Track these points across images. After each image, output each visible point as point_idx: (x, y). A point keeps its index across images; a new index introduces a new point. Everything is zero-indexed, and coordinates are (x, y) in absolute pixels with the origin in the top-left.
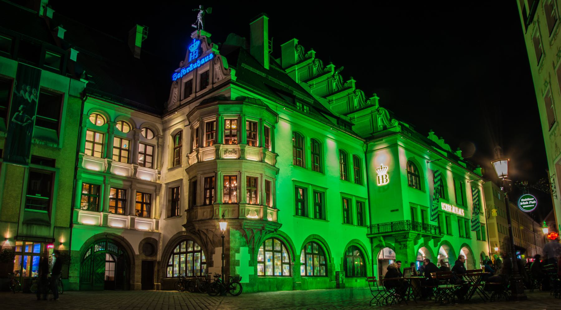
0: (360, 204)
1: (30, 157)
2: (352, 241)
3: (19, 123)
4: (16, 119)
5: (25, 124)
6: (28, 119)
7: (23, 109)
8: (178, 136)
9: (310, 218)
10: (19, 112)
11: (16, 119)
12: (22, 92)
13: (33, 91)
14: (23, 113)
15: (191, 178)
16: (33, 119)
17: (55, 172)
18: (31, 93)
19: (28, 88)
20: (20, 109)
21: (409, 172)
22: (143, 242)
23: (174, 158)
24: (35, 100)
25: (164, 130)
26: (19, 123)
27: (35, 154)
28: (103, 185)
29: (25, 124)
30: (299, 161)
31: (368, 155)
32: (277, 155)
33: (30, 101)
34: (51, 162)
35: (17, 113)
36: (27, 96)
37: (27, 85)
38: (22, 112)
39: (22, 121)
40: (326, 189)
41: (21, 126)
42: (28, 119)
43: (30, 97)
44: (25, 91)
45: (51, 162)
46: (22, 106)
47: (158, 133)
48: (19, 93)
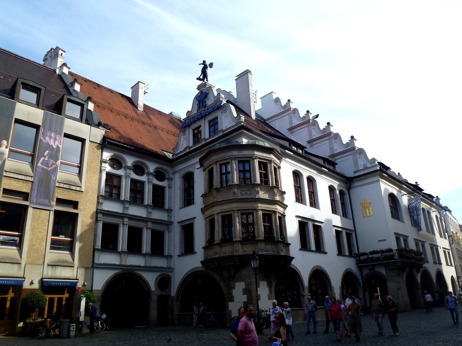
1: (55, 200)
2: (347, 269)
3: (45, 167)
4: (42, 163)
5: (51, 168)
6: (53, 164)
7: (48, 155)
8: (189, 179)
9: (312, 251)
10: (45, 157)
11: (42, 163)
12: (47, 138)
13: (57, 138)
14: (48, 158)
16: (57, 163)
17: (78, 214)
18: (55, 139)
19: (53, 135)
20: (46, 154)
21: (390, 206)
22: (159, 279)
23: (185, 198)
24: (59, 146)
25: (174, 173)
26: (45, 167)
27: (60, 197)
28: (122, 224)
29: (51, 168)
30: (299, 199)
31: (351, 191)
32: (284, 193)
33: (55, 147)
34: (75, 204)
35: (43, 158)
36: (52, 142)
37: (52, 132)
38: (47, 157)
39: (47, 166)
41: (47, 170)
42: (53, 164)
43: (54, 143)
44: (51, 137)
45: (75, 204)
46: (47, 152)
47: (168, 175)
48: (45, 139)
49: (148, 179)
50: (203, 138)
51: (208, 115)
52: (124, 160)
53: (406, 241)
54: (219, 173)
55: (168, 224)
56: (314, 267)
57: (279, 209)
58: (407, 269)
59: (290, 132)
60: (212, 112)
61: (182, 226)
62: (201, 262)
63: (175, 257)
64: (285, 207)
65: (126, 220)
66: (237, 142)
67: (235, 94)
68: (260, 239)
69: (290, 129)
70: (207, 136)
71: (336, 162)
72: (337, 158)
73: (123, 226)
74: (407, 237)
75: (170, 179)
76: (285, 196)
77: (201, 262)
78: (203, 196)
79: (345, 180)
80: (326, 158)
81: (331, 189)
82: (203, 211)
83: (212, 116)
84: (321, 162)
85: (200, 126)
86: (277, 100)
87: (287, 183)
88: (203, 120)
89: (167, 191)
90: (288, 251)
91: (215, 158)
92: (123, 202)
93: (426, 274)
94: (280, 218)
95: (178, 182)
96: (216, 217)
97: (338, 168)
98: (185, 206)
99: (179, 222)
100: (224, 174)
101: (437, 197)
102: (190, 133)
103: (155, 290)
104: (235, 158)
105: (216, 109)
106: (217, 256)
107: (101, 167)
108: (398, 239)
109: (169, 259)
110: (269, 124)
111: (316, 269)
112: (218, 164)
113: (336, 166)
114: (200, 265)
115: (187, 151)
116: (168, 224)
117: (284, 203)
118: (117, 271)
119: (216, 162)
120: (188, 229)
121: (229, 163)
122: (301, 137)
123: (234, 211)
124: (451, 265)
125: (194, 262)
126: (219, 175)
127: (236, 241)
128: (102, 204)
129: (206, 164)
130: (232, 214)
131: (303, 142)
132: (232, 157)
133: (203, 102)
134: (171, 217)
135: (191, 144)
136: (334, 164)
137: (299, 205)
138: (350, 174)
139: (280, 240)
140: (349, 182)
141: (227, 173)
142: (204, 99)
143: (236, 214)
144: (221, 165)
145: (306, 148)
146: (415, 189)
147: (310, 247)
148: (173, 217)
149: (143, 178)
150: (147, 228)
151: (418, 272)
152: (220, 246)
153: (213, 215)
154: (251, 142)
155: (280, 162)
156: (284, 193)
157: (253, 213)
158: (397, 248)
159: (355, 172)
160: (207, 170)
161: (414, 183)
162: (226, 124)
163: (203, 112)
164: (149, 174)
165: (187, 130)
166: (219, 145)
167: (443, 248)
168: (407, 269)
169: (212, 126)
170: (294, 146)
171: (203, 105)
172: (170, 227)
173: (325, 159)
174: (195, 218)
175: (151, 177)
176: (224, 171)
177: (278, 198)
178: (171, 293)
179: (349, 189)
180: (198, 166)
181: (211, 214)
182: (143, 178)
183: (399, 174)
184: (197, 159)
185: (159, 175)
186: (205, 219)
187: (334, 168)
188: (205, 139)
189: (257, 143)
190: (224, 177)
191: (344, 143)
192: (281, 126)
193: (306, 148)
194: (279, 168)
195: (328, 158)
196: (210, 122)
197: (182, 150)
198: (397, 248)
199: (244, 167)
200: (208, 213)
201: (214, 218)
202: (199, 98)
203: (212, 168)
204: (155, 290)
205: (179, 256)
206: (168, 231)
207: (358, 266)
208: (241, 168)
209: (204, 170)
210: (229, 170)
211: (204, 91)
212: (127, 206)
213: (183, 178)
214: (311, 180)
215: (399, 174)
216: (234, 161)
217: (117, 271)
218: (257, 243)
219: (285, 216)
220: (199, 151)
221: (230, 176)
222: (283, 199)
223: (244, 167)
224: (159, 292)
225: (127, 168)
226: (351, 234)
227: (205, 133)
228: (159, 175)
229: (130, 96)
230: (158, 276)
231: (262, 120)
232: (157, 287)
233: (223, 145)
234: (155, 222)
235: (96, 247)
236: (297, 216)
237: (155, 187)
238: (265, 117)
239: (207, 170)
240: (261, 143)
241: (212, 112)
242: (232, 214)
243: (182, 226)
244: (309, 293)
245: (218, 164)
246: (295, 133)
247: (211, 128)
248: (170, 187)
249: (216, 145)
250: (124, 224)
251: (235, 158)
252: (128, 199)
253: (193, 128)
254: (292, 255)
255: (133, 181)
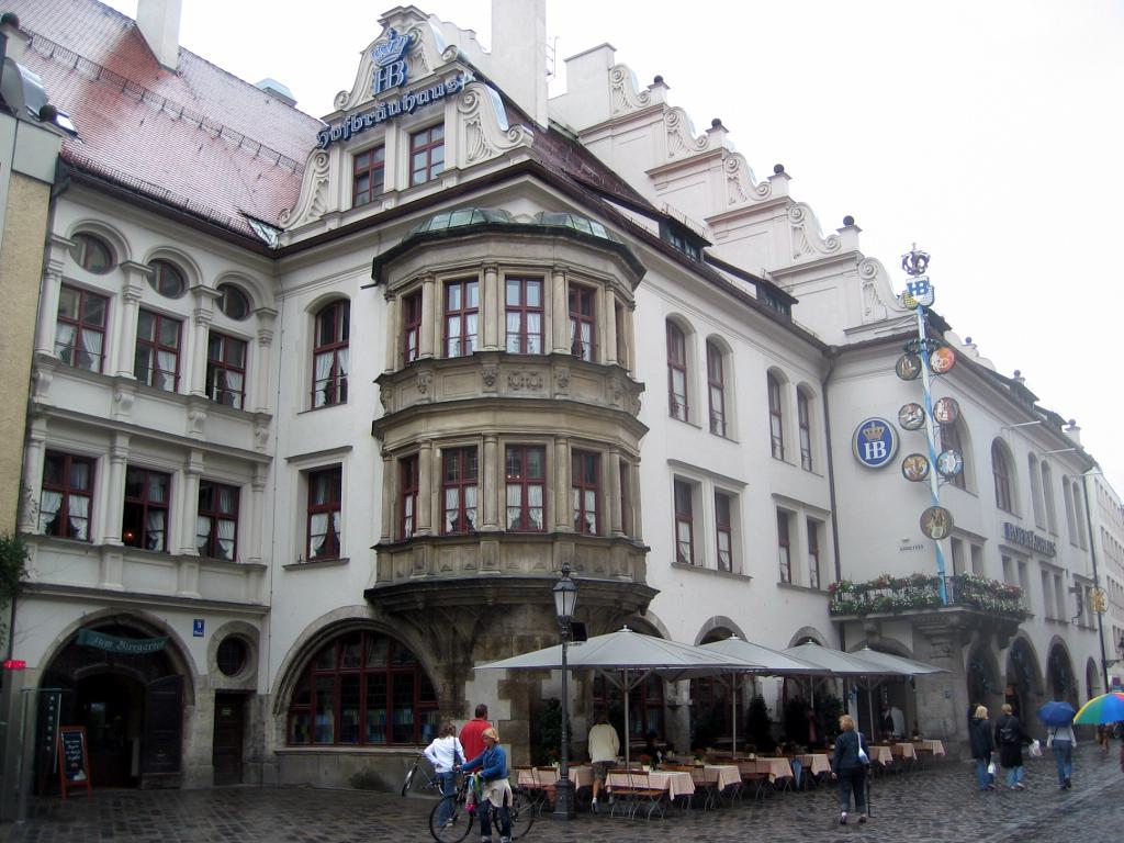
0: (813, 526)
8: (331, 318)
9: (710, 572)
15: (389, 448)
25: (280, 295)
28: (106, 458)
30: (678, 407)
31: (836, 391)
32: (641, 387)
40: (742, 485)
49: (197, 311)
50: (388, 186)
51: (412, 112)
52: (120, 241)
53: (976, 551)
54: (439, 307)
55: (255, 464)
56: (711, 619)
57: (623, 436)
58: (975, 636)
59: (653, 182)
60: (425, 104)
61: (301, 471)
62: (368, 594)
63: (276, 571)
64: (640, 430)
65: (122, 442)
66: (506, 214)
67: (485, 39)
68: (560, 529)
69: (653, 174)
70: (403, 185)
71: (793, 294)
72: (797, 280)
73: (112, 463)
74: (983, 539)
75: (269, 315)
76: (643, 397)
77: (368, 594)
78: (381, 380)
79: (818, 353)
80: (767, 282)
81: (775, 380)
82: (379, 429)
83: (427, 116)
84: (751, 290)
85: (382, 146)
86: (618, 74)
87: (649, 360)
88: (394, 128)
89: (255, 354)
90: (642, 568)
91: (430, 260)
92: (115, 383)
93: (1023, 651)
94: (623, 466)
95: (296, 324)
96: (424, 454)
97: (799, 315)
98: (313, 408)
99: (290, 460)
100: (456, 314)
101: (1072, 423)
102: (341, 168)
103: (206, 672)
104: (497, 267)
105: (440, 98)
106: (422, 577)
107: (46, 260)
108: (955, 544)
109: (253, 577)
110: (588, 147)
111: (715, 626)
112: (440, 280)
113: (793, 307)
114: (363, 602)
115: (333, 225)
116: (255, 464)
117: (638, 418)
118: (90, 610)
119: (432, 276)
120: (323, 485)
121: (475, 279)
122: (691, 202)
123: (485, 437)
124: (1092, 629)
125: (342, 593)
126: (439, 316)
127: (485, 534)
128: (46, 384)
129: (398, 276)
130: (476, 447)
131: (697, 224)
132: (488, 260)
133: (395, 68)
134: (265, 439)
135: (346, 205)
136: (787, 301)
137: (677, 427)
138: (833, 336)
139: (621, 535)
140: (830, 361)
141: (466, 312)
142: (400, 58)
143: (491, 447)
144: (447, 284)
145: (710, 245)
146: (1011, 397)
147: (703, 561)
148: (271, 441)
149: (181, 306)
150: (188, 473)
151: (1002, 647)
152: (434, 546)
153: (415, 443)
154: (552, 219)
155: (634, 288)
156: (641, 387)
157: (543, 448)
158: (952, 575)
159: (848, 332)
160: (399, 297)
161: (1011, 376)
162: (472, 153)
163: (395, 102)
164: (198, 292)
165: (335, 155)
166: (445, 217)
167: (1074, 575)
168: (975, 636)
169: (421, 150)
170: (676, 235)
171: (394, 78)
172: (260, 471)
173: (764, 286)
174: (347, 449)
175: (207, 304)
176: (456, 305)
177: (620, 405)
178: (256, 684)
179: (826, 383)
180: (367, 278)
181: (410, 441)
182: (181, 306)
183: (969, 340)
184: (368, 257)
185: (235, 299)
186: (385, 455)
187: (788, 312)
188: (396, 193)
189: (569, 224)
190: (455, 324)
191: (825, 236)
192: (628, 158)
193: (710, 245)
194: (632, 306)
195: (768, 277)
196: (413, 136)
197: (311, 220)
198: (952, 575)
199: (523, 296)
200: (395, 438)
201: (416, 456)
202: (381, 53)
203: (419, 293)
204: (206, 672)
205: (289, 568)
206: (255, 486)
207: (834, 623)
208: (514, 301)
209: (389, 296)
210: (474, 302)
211: (399, 31)
212: (126, 396)
213: (311, 312)
214: (716, 350)
215: (969, 340)
216: (491, 276)
217: (90, 610)
218: (553, 543)
219: (639, 460)
220: (374, 230)
221: (472, 321)
222: (638, 405)
223: (523, 296)
224: (224, 682)
225: (127, 268)
226: (823, 522)
227: (395, 174)
228: (235, 299)
229: (133, 17)
230: (220, 629)
231: (567, 135)
232: (216, 665)
233: (461, 219)
234: (214, 453)
235: (26, 530)
236: (672, 463)
237: (215, 337)
238: (578, 125)
239: (399, 297)
240: (580, 225)
241: (425, 104)
242: (476, 447)
243: (301, 471)
244: (691, 698)
245: (440, 280)
246: (671, 187)
247: (417, 158)
248: (265, 341)
249: (436, 218)
250: (113, 458)
251: (497, 267)
252: (128, 370)
253: (356, 152)
254: (650, 584)
255: (146, 313)
